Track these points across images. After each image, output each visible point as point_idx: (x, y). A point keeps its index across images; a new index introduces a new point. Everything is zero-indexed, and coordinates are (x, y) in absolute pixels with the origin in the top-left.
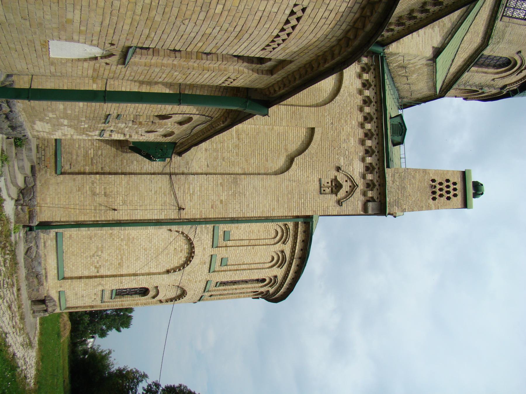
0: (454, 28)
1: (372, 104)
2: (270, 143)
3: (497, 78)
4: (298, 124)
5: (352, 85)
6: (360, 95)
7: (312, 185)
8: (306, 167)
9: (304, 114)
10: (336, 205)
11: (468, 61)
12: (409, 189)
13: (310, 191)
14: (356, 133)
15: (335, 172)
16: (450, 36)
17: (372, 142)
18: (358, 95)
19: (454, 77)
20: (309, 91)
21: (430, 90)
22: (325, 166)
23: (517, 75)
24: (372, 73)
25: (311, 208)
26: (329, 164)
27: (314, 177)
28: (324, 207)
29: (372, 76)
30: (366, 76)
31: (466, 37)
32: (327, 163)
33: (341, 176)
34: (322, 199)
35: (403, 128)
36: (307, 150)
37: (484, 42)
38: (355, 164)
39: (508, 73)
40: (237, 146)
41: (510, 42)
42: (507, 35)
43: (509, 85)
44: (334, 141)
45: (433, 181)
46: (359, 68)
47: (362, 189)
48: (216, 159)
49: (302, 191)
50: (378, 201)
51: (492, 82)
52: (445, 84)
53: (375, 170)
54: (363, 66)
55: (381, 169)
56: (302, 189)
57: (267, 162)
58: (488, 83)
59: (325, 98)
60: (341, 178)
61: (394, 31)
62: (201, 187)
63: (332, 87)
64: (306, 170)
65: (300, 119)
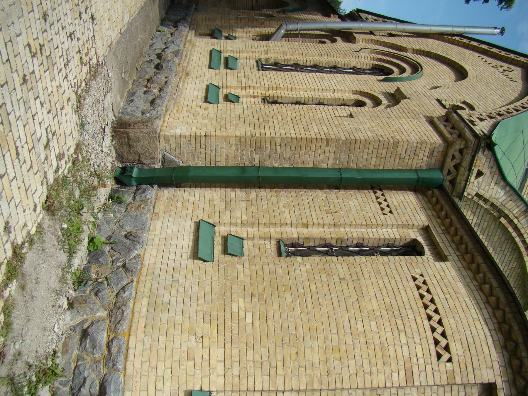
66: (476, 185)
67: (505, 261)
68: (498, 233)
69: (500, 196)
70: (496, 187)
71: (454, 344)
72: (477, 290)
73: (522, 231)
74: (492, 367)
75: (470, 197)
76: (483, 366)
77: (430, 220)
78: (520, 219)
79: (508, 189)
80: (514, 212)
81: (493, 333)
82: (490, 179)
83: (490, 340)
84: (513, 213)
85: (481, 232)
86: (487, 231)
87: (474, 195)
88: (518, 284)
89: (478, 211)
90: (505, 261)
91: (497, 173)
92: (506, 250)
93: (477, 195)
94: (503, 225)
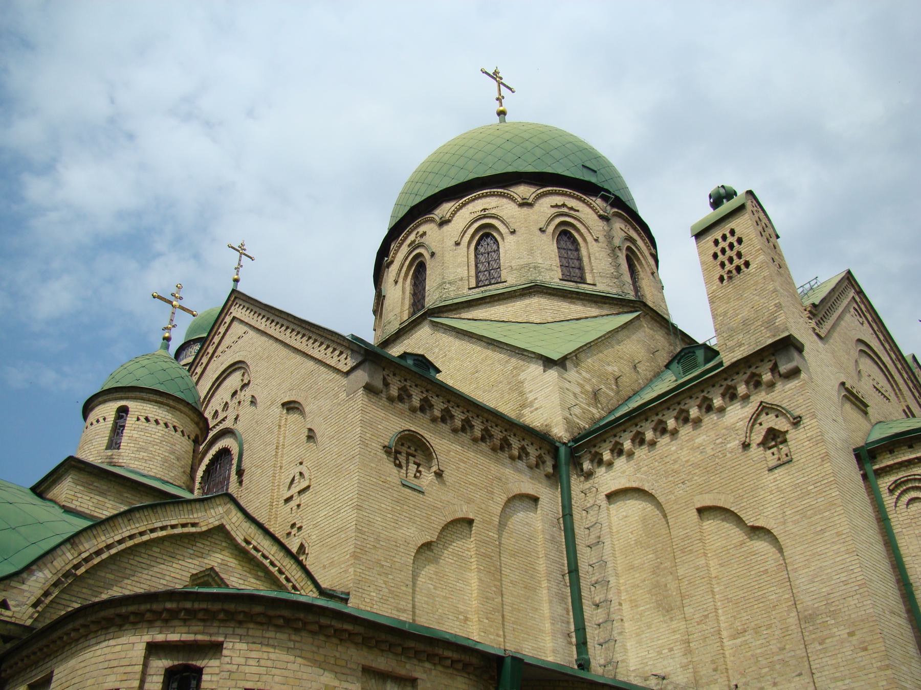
0: (515, 352)
1: (639, 430)
2: (738, 574)
3: (592, 236)
4: (698, 538)
5: (624, 472)
6: (634, 453)
7: (782, 480)
8: (758, 502)
9: (680, 534)
10: (802, 426)
11: (571, 298)
12: (745, 313)
13: (792, 480)
14: (687, 438)
15: (751, 449)
16: (525, 353)
17: (691, 407)
18: (635, 457)
19: (605, 303)
20: (650, 536)
21: (641, 326)
22: (748, 470)
23: (578, 211)
24: (600, 447)
25: (819, 469)
26: (743, 464)
27: (769, 482)
28: (811, 445)
29: (604, 445)
30: (607, 456)
31: (535, 322)
32: (742, 468)
33: (755, 437)
34: (799, 454)
35: (683, 354)
36: (732, 509)
37: (534, 292)
38: (732, 421)
39: (578, 225)
40: (757, 630)
41: (531, 252)
42: (522, 262)
43: (596, 213)
44: (708, 469)
45: (721, 279)
46: (600, 469)
47: (766, 392)
48: (784, 662)
49: (796, 494)
50: (773, 358)
51: (601, 239)
52: (621, 310)
53: (730, 383)
54: (595, 464)
55: (725, 376)
56: (793, 495)
57: (769, 571)
58: (604, 245)
59: (653, 507)
60: (758, 436)
61: (523, 446)
62: (836, 679)
63: (636, 502)
64: (762, 501)
65: (690, 537)
66: (19, 608)
67: (148, 562)
68: (103, 574)
69: (43, 577)
70: (29, 583)
71: (106, 684)
72: (106, 634)
73: (102, 545)
74: (134, 644)
75: (36, 615)
76: (130, 654)
77: (22, 683)
78: (83, 550)
79: (34, 567)
80: (71, 557)
81: (108, 636)
82: (15, 591)
83: (112, 642)
84: (72, 559)
85: (96, 597)
86: (96, 589)
87: (34, 610)
88: (189, 543)
89: (63, 602)
90: (148, 562)
91: (8, 581)
92: (131, 562)
93: (35, 605)
94: (86, 572)
